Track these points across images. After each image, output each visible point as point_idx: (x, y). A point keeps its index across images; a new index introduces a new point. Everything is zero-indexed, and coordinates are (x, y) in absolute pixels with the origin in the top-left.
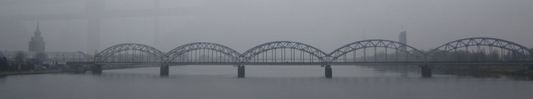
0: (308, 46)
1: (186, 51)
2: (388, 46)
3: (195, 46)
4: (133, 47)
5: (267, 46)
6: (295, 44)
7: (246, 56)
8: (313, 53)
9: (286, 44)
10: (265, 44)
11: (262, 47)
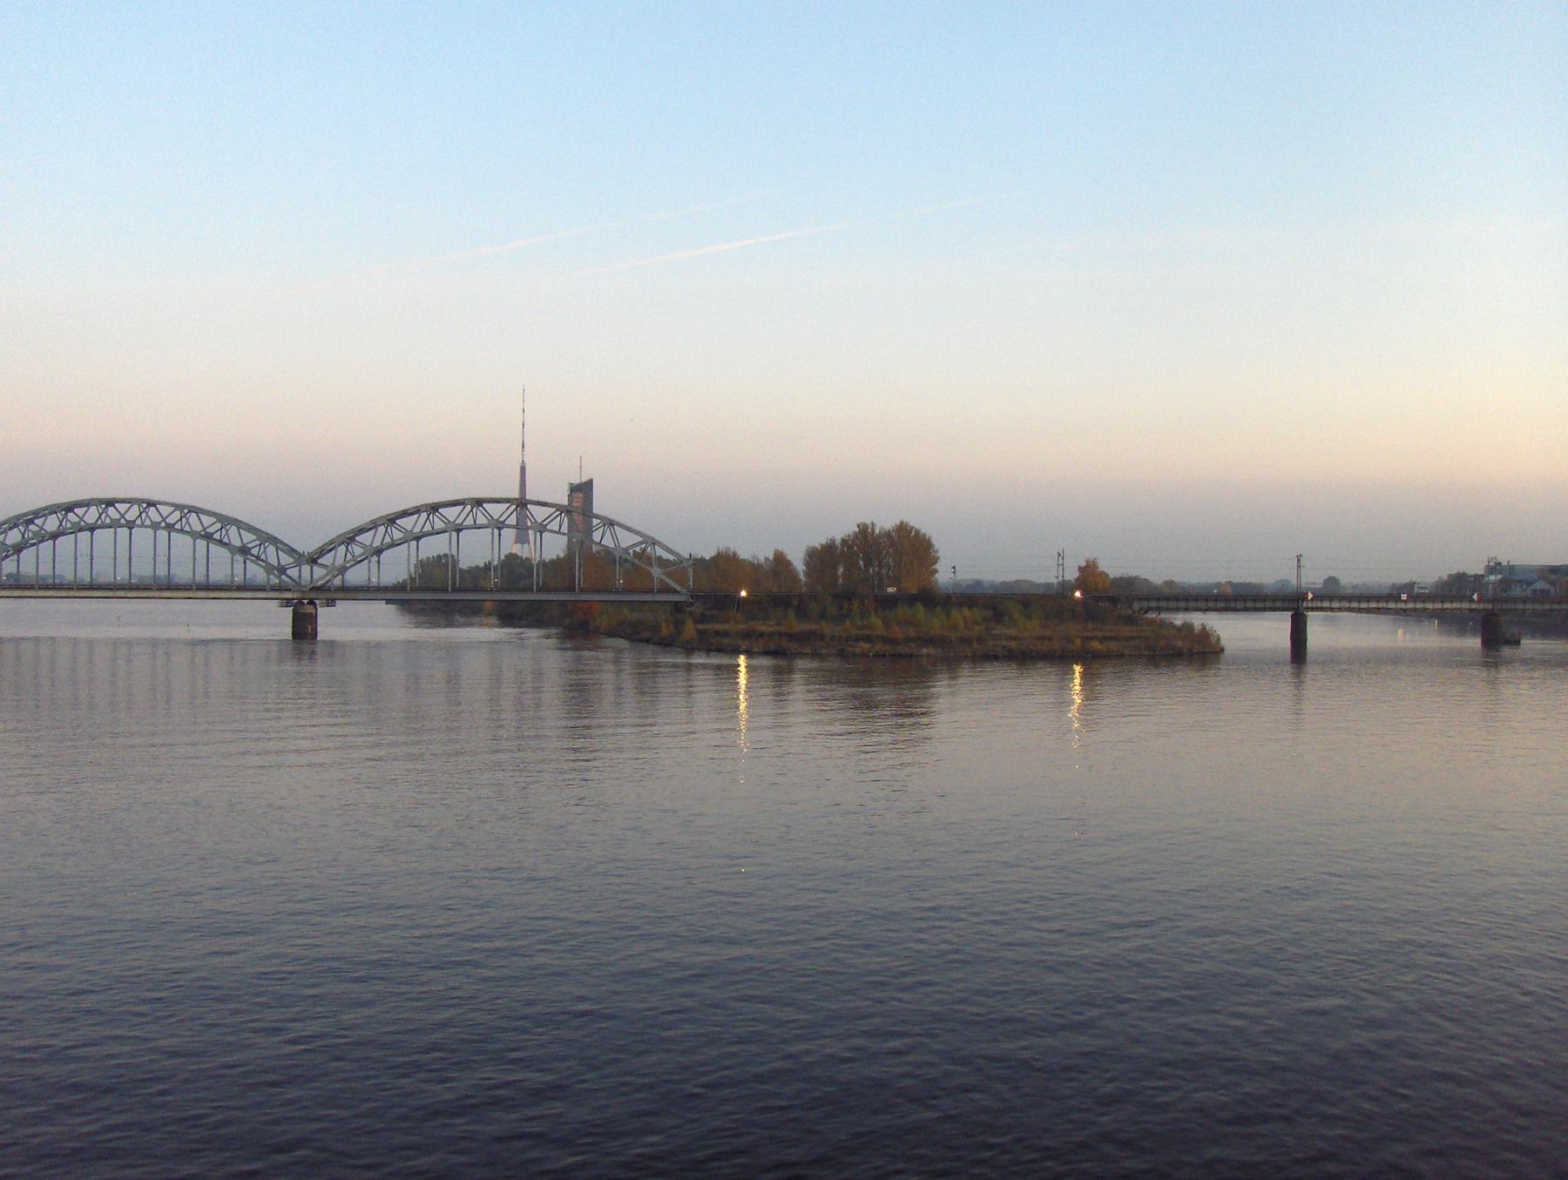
0: (226, 521)
2: (548, 527)
6: (172, 508)
8: (244, 550)
9: (135, 510)
10: (46, 509)
11: (36, 521)
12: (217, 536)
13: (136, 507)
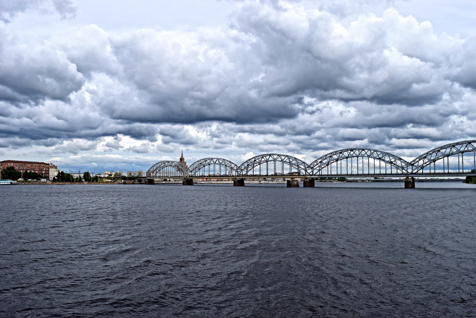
3: (346, 154)
4: (267, 159)
5: (448, 150)
7: (416, 164)
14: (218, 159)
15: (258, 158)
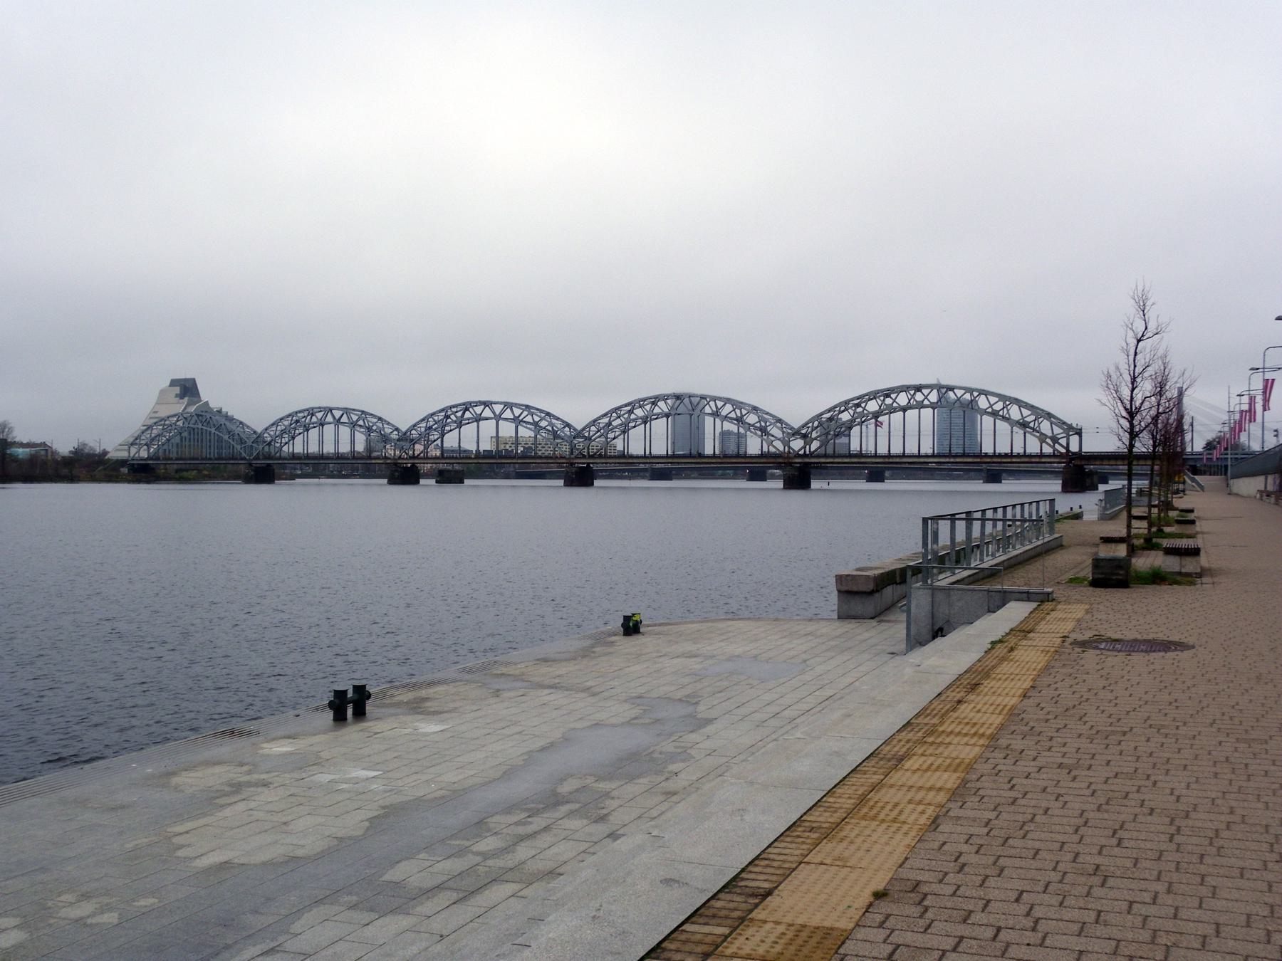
1: (870, 416)
6: (964, 391)
12: (1001, 413)
13: (935, 391)
14: (347, 411)
15: (454, 410)
